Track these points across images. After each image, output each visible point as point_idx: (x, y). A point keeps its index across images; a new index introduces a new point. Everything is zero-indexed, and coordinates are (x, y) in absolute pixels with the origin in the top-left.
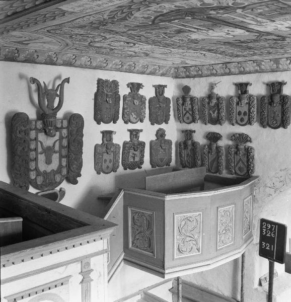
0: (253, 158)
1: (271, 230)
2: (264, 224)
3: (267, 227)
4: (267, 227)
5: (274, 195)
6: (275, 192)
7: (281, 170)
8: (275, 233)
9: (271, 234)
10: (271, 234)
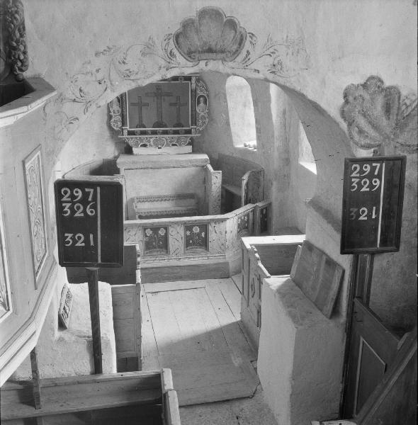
0: (22, 29)
1: (84, 201)
2: (66, 192)
3: (73, 197)
4: (73, 197)
5: (83, 118)
6: (86, 110)
7: (97, 54)
8: (94, 207)
9: (84, 211)
10: (84, 211)
